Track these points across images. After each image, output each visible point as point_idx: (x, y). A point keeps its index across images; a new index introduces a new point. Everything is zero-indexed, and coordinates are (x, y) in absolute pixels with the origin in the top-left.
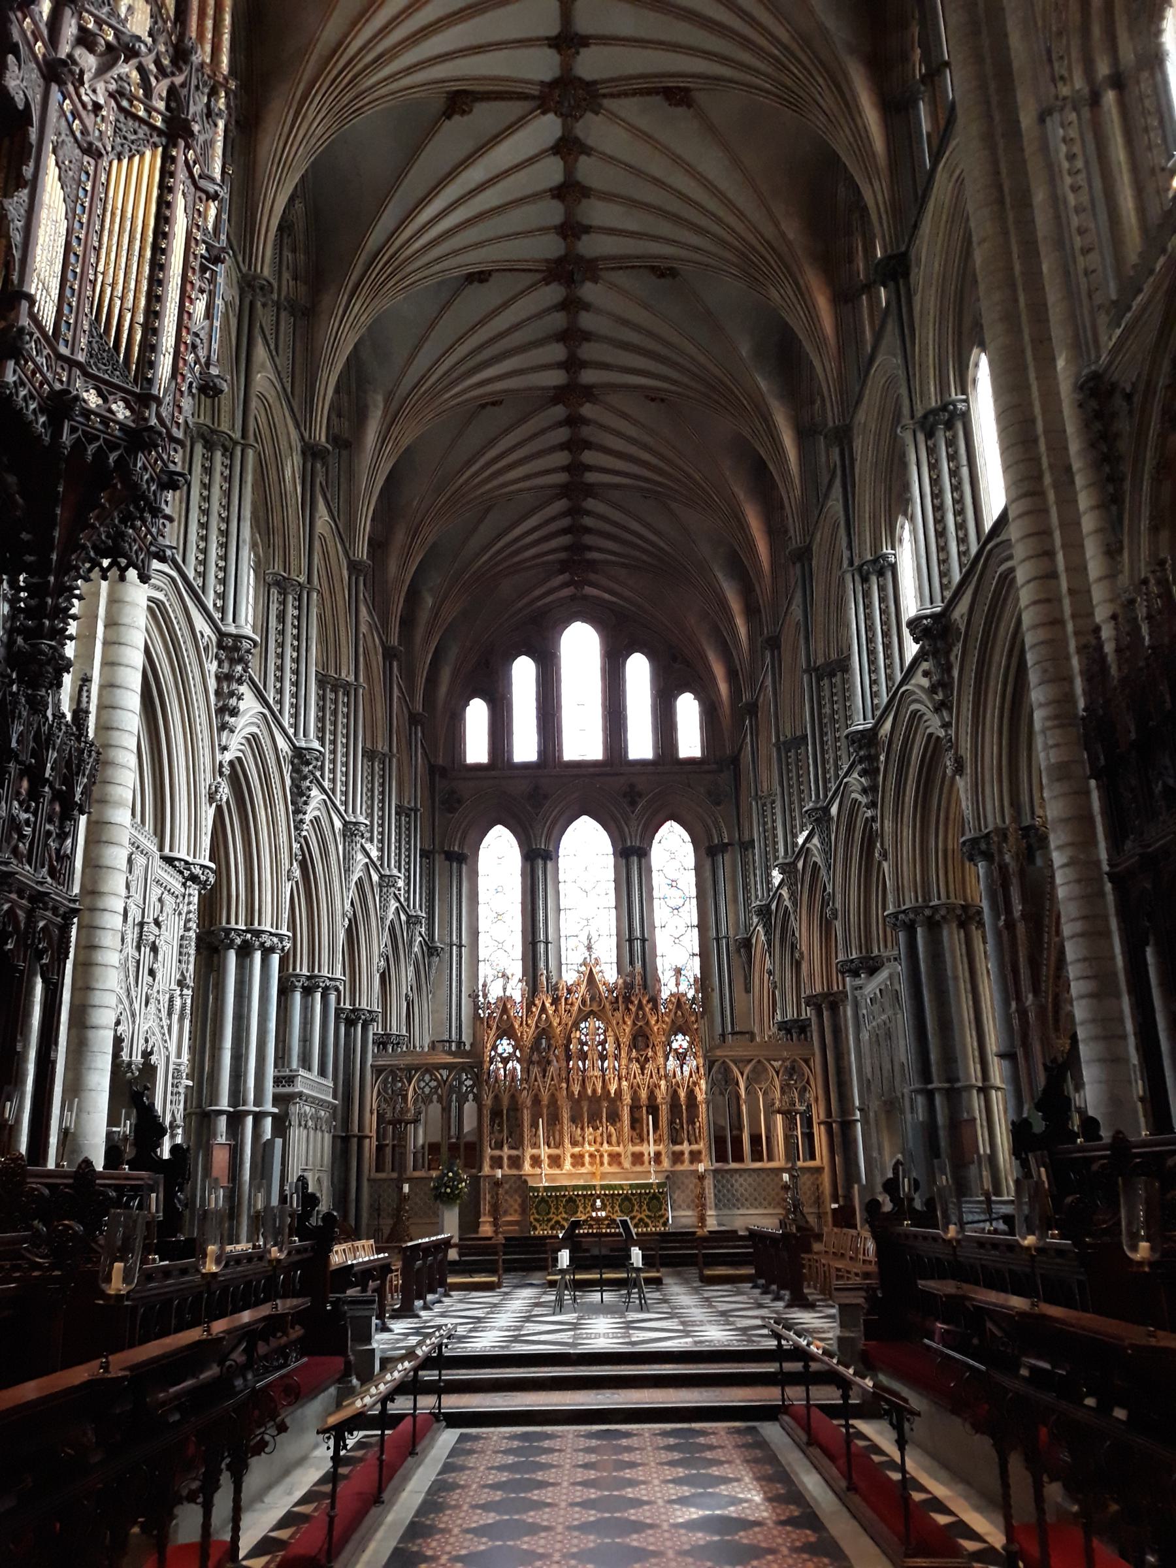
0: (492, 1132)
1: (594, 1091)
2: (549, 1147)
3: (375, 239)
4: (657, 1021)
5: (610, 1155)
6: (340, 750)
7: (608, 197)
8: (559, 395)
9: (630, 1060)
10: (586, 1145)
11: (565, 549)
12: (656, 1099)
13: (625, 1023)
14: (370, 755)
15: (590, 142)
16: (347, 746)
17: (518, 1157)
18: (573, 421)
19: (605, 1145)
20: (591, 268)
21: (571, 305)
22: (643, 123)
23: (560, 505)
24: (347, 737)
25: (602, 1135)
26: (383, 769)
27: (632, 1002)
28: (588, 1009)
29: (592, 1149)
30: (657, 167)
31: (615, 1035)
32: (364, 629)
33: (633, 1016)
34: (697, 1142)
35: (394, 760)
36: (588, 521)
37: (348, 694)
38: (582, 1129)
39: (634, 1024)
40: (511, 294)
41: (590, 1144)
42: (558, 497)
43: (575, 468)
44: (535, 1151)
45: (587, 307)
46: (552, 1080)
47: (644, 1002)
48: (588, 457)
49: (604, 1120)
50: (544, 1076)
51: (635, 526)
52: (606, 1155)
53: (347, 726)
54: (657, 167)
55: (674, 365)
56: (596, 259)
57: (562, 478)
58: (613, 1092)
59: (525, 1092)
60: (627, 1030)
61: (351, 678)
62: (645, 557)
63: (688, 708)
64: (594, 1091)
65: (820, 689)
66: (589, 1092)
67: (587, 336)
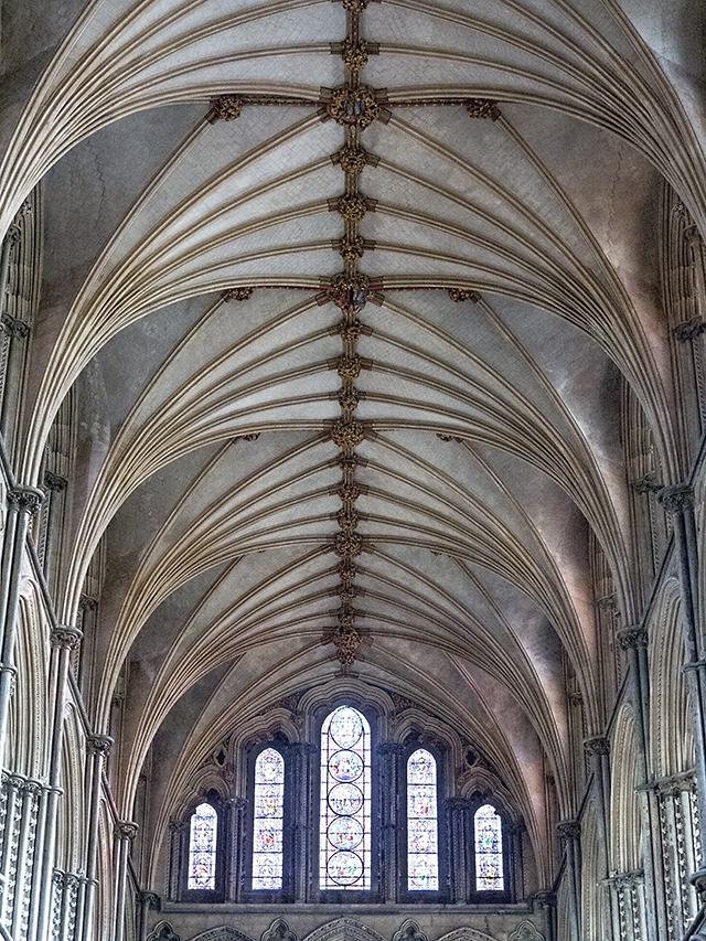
3: (116, 250)
6: (24, 874)
7: (398, 210)
8: (330, 431)
11: (331, 613)
14: (63, 881)
15: (379, 150)
16: (33, 870)
18: (347, 461)
20: (376, 288)
21: (349, 327)
22: (440, 134)
23: (330, 559)
24: (35, 858)
26: (77, 900)
30: (459, 181)
32: (66, 714)
35: (93, 888)
36: (360, 580)
37: (39, 801)
40: (274, 315)
42: (324, 549)
43: (347, 515)
45: (369, 331)
48: (363, 503)
51: (421, 588)
53: (35, 844)
54: (459, 181)
55: (474, 401)
56: (381, 278)
57: (331, 527)
61: (45, 781)
62: (435, 629)
63: (487, 823)
65: (661, 813)
67: (368, 364)
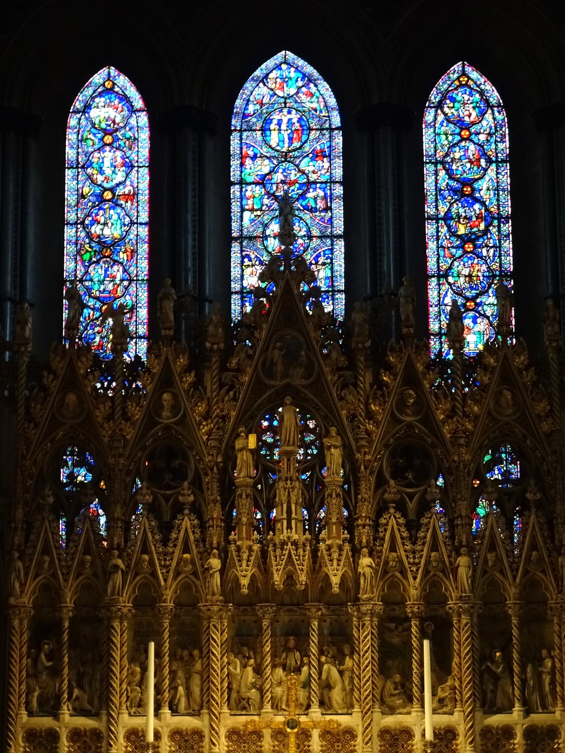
0: (33, 674)
1: (290, 578)
2: (174, 711)
4: (451, 414)
5: (325, 734)
9: (381, 510)
10: (268, 708)
12: (444, 600)
13: (370, 415)
17: (96, 735)
19: (316, 712)
25: (306, 685)
27: (389, 368)
28: (278, 383)
29: (280, 719)
31: (346, 447)
33: (392, 400)
34: (545, 708)
38: (258, 671)
39: (395, 420)
41: (276, 707)
44: (136, 722)
46: (186, 549)
47: (420, 367)
49: (314, 649)
50: (165, 542)
52: (315, 734)
58: (335, 580)
59: (118, 577)
60: (377, 433)
64: (290, 578)
66: (278, 578)
